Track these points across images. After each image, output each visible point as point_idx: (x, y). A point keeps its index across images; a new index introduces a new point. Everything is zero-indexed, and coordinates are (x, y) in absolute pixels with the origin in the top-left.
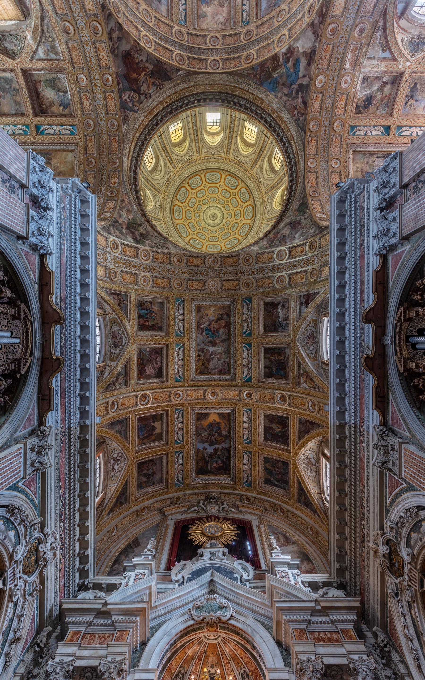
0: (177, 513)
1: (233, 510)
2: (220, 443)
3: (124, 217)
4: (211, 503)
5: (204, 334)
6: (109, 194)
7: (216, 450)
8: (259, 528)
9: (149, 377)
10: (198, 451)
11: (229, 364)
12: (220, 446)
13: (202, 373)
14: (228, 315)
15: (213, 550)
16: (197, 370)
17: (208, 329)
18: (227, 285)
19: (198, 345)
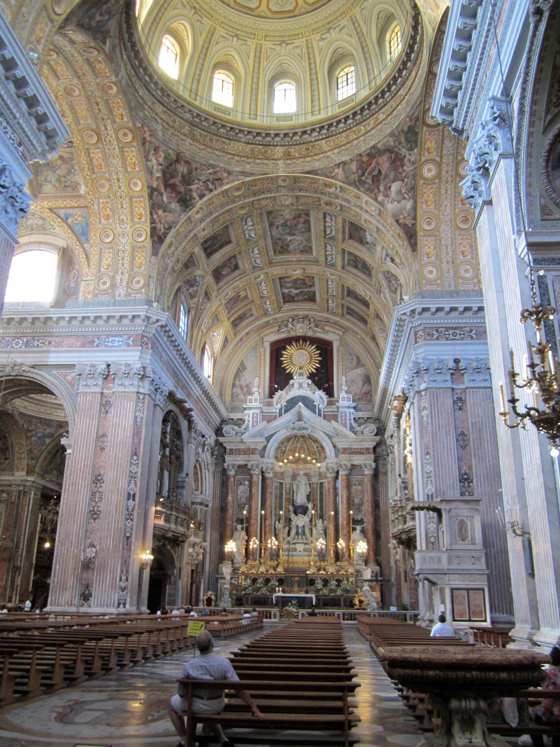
0: (271, 333)
1: (319, 330)
2: (306, 288)
3: (155, 167)
4: (299, 322)
5: (280, 228)
6: (120, 135)
7: (301, 292)
8: (338, 352)
9: (227, 275)
10: (283, 294)
11: (311, 248)
12: (306, 290)
13: (281, 253)
14: (308, 215)
15: (301, 381)
16: (275, 252)
17: (284, 225)
18: (304, 200)
19: (272, 237)
